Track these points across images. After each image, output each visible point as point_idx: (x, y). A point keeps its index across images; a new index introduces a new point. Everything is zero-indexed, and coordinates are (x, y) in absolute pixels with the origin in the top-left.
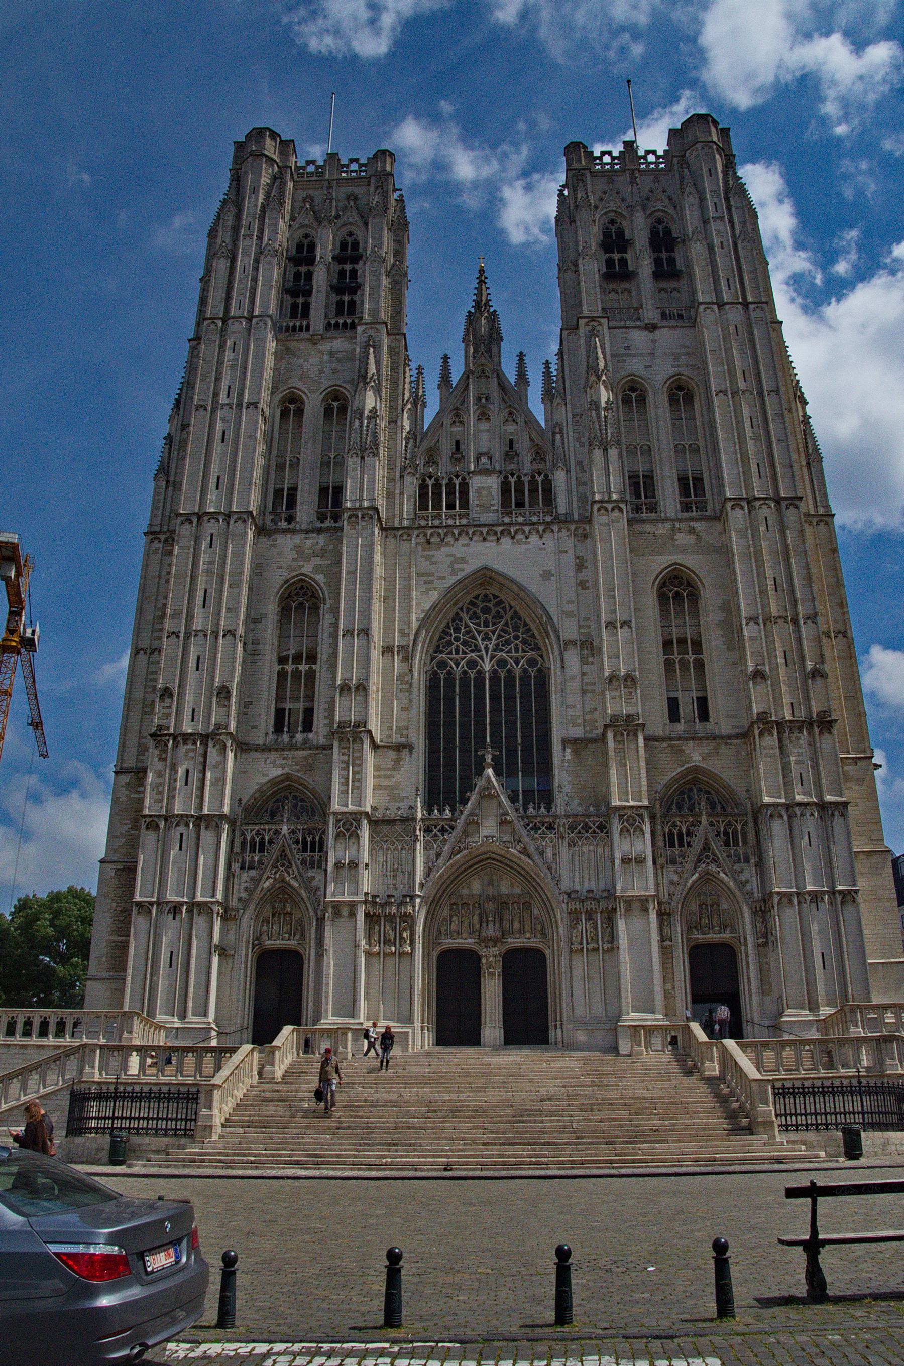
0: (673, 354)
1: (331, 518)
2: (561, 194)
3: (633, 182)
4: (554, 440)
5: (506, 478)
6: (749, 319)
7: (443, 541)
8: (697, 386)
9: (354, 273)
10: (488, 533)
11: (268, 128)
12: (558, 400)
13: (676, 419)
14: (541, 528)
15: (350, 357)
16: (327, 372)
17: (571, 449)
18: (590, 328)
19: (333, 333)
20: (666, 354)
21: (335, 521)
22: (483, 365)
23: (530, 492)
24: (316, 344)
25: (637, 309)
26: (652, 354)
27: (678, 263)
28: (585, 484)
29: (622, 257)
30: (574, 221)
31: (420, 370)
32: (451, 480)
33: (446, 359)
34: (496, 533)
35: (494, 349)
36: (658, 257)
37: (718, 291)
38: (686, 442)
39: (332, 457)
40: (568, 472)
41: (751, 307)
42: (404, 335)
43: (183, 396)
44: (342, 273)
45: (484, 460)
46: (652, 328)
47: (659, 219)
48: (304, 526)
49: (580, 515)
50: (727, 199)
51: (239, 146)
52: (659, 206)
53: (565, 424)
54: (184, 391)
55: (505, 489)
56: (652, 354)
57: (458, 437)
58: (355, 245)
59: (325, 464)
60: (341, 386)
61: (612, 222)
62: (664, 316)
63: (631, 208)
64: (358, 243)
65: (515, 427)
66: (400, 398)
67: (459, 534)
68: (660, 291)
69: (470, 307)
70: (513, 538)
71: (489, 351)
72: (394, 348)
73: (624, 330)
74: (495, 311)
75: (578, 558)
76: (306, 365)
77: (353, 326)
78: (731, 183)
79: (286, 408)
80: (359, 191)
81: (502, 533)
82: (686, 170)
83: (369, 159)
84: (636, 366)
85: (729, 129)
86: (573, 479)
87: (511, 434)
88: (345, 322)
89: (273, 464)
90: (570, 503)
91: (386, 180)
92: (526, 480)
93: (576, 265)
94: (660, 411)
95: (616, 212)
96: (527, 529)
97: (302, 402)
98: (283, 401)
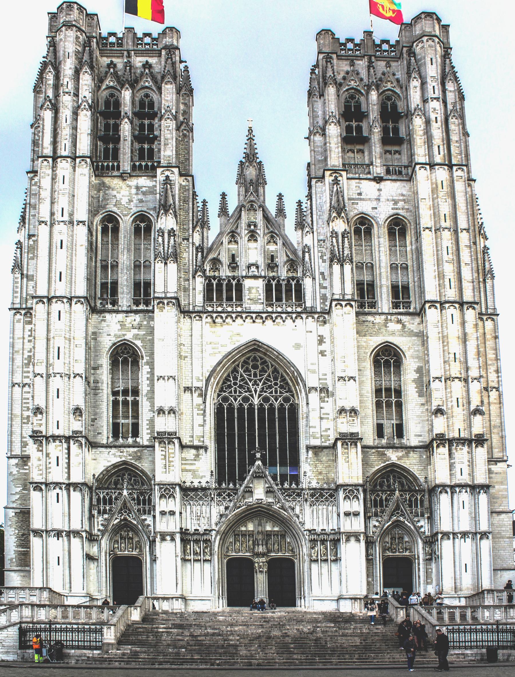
0: (393, 200)
1: (144, 303)
2: (313, 72)
3: (370, 65)
4: (304, 257)
5: (269, 281)
6: (452, 176)
7: (224, 321)
8: (410, 223)
9: (151, 127)
10: (256, 318)
11: (76, 3)
12: (307, 229)
13: (392, 246)
14: (294, 316)
15: (152, 191)
16: (135, 201)
17: (316, 263)
18: (333, 178)
19: (137, 173)
20: (388, 200)
21: (147, 306)
22: (252, 201)
23: (286, 291)
24: (125, 180)
25: (368, 166)
26: (378, 200)
27: (400, 132)
28: (325, 288)
29: (359, 125)
30: (323, 95)
31: (204, 202)
32: (229, 281)
33: (224, 196)
34: (262, 318)
35: (261, 190)
36: (386, 126)
37: (430, 154)
38: (399, 261)
39: (142, 262)
40: (314, 279)
41: (455, 168)
42: (193, 176)
43: (27, 214)
44: (142, 126)
45: (253, 269)
46: (378, 180)
47: (388, 97)
48: (125, 308)
49: (321, 308)
50: (443, 84)
51: (53, 17)
52: (389, 86)
53: (312, 246)
54: (27, 210)
55: (268, 288)
56: (378, 200)
57: (234, 252)
58: (151, 105)
59: (137, 267)
60: (146, 212)
61: (352, 97)
62: (388, 172)
63: (369, 88)
64: (153, 103)
65: (276, 247)
66: (191, 222)
67: (236, 318)
68: (386, 152)
69: (241, 157)
70: (274, 321)
71: (257, 191)
72: (185, 186)
73: (357, 181)
74: (261, 162)
75: (319, 336)
76: (119, 196)
77: (154, 168)
78: (447, 70)
79: (105, 225)
80: (153, 61)
81: (266, 318)
82: (412, 59)
83: (159, 34)
84: (364, 207)
85: (449, 26)
86: (317, 284)
87: (272, 251)
88: (147, 164)
89: (99, 264)
90: (314, 299)
91: (174, 53)
92: (284, 283)
93: (324, 129)
94: (382, 240)
95: (356, 90)
96: (284, 316)
97: (118, 222)
98: (103, 220)
